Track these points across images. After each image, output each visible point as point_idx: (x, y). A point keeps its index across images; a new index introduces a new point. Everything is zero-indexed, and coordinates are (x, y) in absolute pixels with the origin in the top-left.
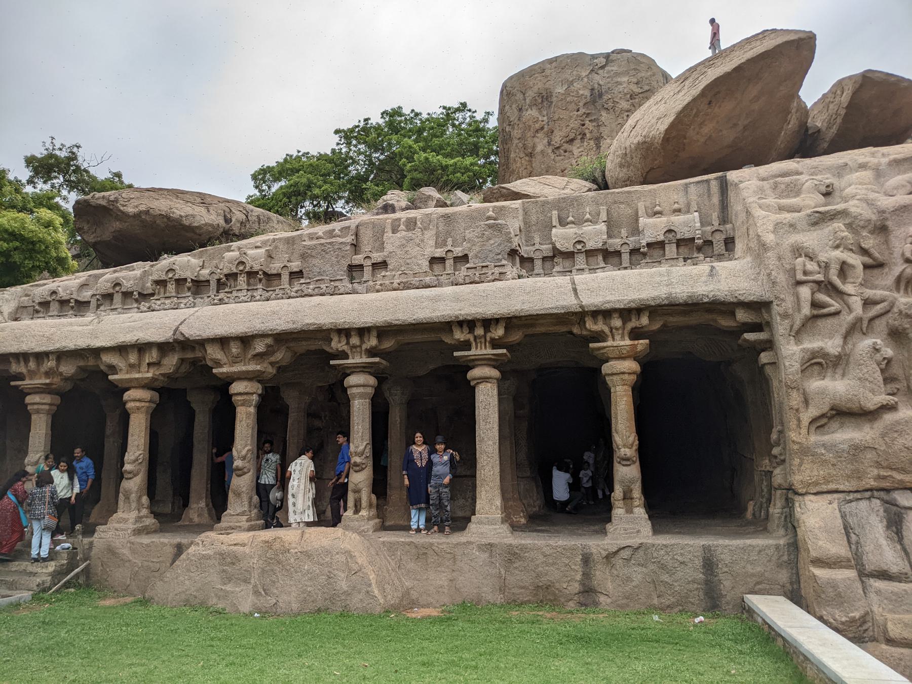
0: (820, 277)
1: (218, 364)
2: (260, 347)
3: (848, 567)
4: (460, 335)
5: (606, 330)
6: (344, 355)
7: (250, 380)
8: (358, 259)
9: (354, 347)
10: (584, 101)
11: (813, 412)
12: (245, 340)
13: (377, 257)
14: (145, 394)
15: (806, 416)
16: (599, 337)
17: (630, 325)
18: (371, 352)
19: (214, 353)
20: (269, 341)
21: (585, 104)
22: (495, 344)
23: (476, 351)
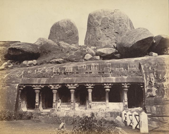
0: (150, 80)
1: (69, 87)
2: (76, 85)
3: (150, 113)
4: (105, 85)
5: (124, 85)
6: (88, 86)
7: (73, 89)
8: (87, 71)
9: (90, 85)
10: (109, 20)
11: (148, 96)
12: (74, 84)
13: (90, 71)
14: (56, 91)
15: (147, 97)
16: (123, 86)
17: (127, 84)
18: (92, 86)
19: (68, 85)
20: (77, 84)
21: (109, 21)
22: (110, 86)
23: (107, 87)
